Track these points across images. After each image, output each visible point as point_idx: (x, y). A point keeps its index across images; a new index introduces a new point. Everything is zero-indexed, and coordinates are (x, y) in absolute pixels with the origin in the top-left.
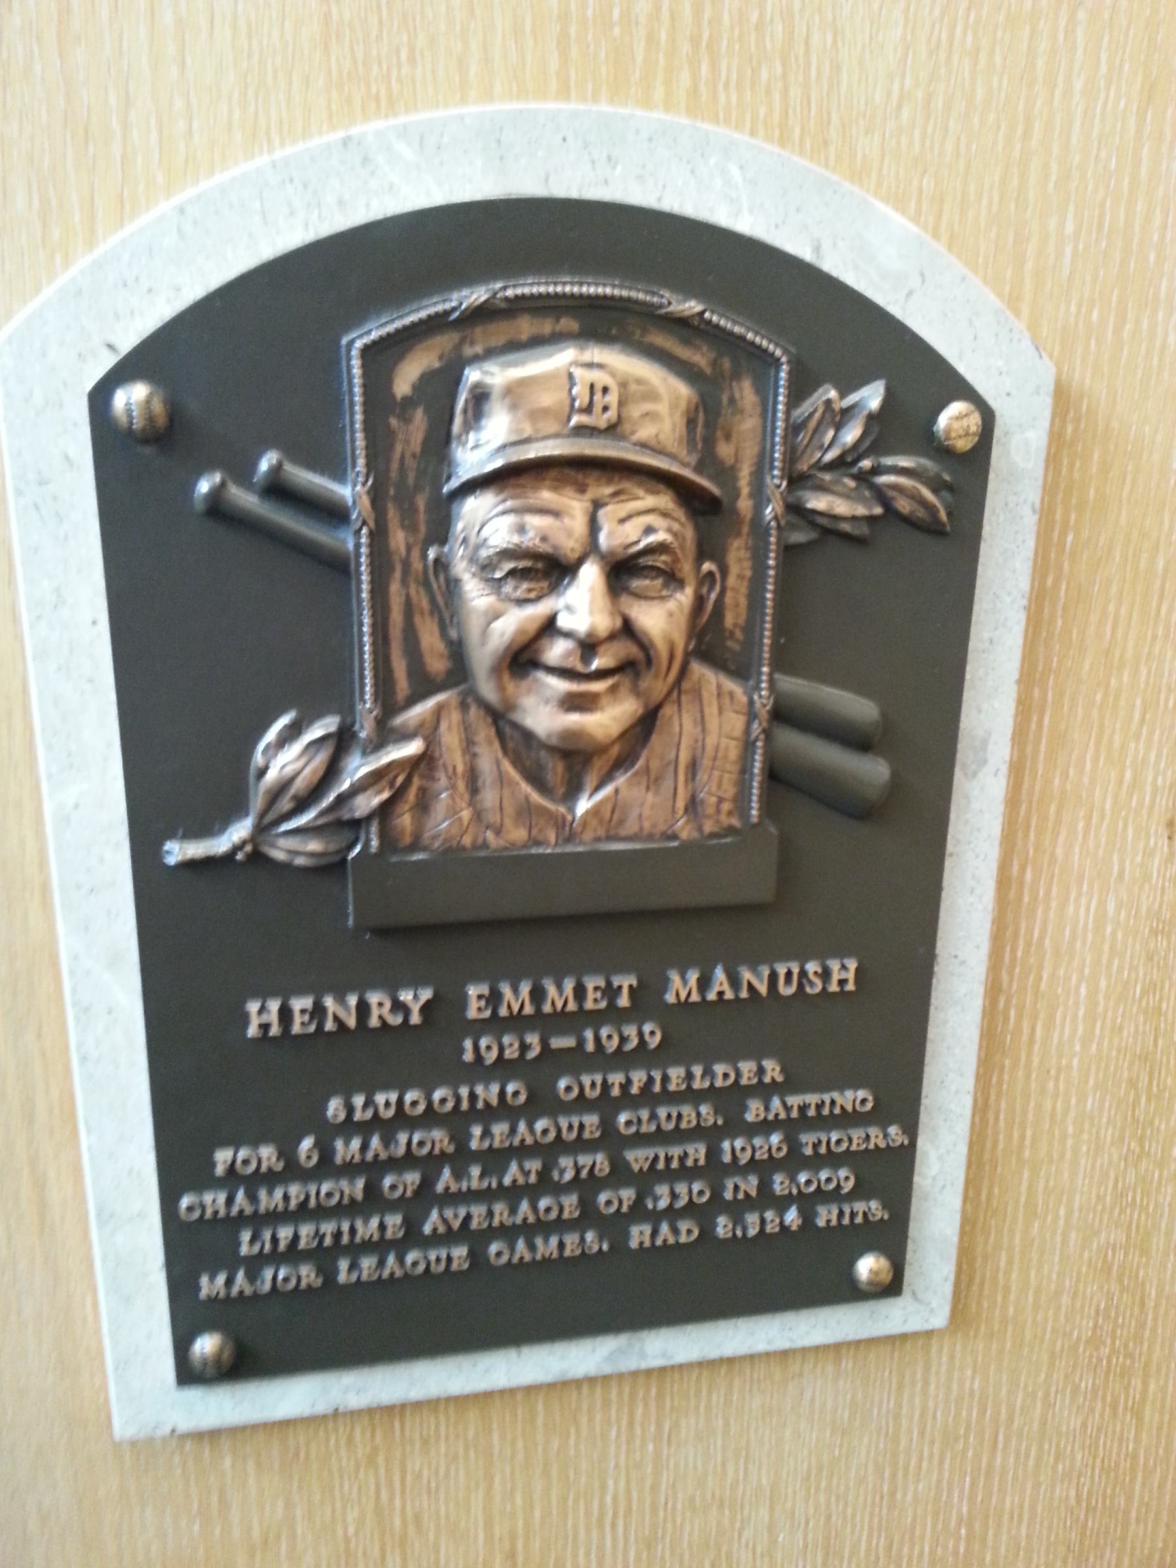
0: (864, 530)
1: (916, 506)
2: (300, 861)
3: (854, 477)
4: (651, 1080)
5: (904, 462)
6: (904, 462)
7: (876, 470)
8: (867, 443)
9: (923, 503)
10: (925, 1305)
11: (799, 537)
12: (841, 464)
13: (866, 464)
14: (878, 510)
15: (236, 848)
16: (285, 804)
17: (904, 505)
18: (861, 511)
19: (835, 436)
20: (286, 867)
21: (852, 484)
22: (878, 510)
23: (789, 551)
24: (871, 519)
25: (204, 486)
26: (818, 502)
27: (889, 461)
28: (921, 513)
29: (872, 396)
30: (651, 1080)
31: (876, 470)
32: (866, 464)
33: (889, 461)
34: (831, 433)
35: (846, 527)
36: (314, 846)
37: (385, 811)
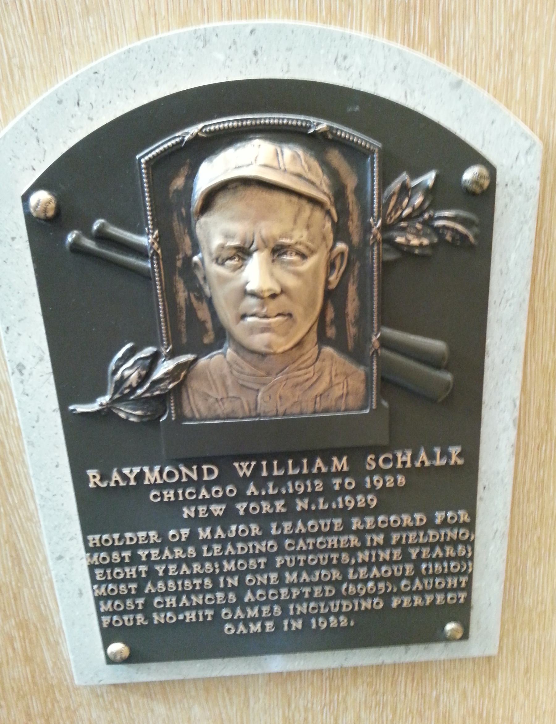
0: (428, 252)
2: (132, 419)
3: (419, 223)
4: (401, 538)
5: (447, 213)
6: (447, 213)
7: (432, 218)
10: (475, 647)
11: (390, 256)
13: (426, 216)
20: (126, 421)
21: (419, 226)
22: (436, 240)
25: (71, 238)
27: (437, 214)
30: (401, 538)
32: (426, 216)
33: (437, 214)
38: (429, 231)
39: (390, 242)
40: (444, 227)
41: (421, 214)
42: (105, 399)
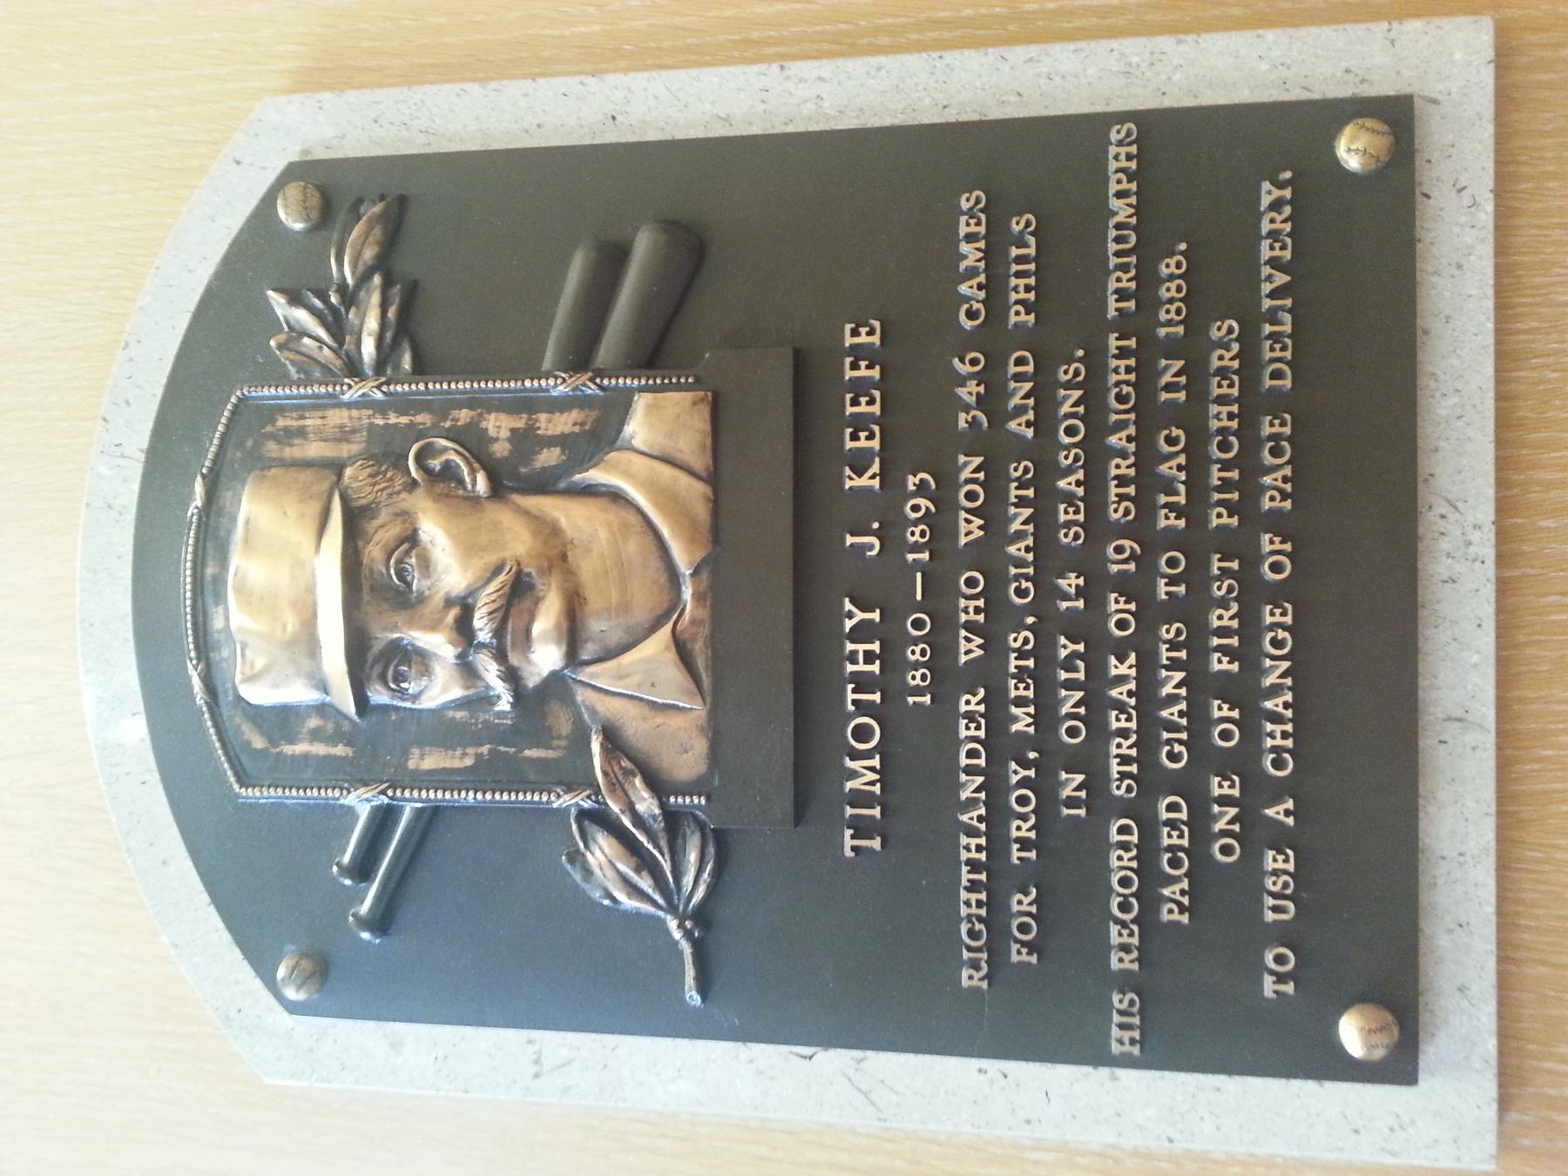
0: (396, 290)
1: (371, 239)
3: (347, 312)
8: (317, 303)
9: (367, 234)
11: (407, 362)
12: (336, 324)
13: (334, 299)
15: (688, 934)
16: (645, 883)
17: (369, 254)
18: (376, 298)
19: (310, 336)
22: (377, 279)
23: (421, 369)
24: (387, 286)
26: (368, 349)
28: (377, 232)
29: (277, 301)
31: (342, 289)
34: (306, 340)
35: (391, 314)
36: (693, 857)
37: (657, 785)
38: (362, 294)
39: (380, 366)
40: (354, 266)
42: (672, 924)
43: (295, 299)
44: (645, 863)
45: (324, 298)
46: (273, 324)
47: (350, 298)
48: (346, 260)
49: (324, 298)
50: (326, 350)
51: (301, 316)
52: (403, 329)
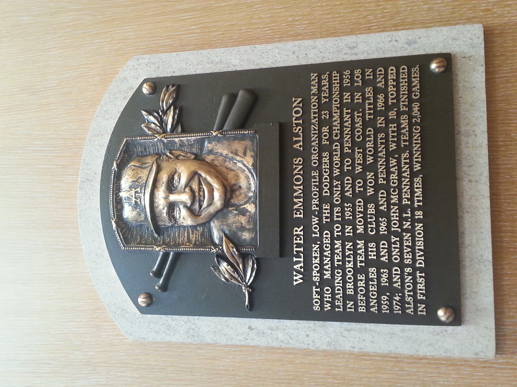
8: (156, 114)
13: (161, 114)
14: (172, 107)
16: (236, 276)
22: (172, 107)
26: (169, 126)
35: (176, 117)
40: (167, 104)
41: (160, 116)
43: (150, 114)
44: (235, 270)
45: (158, 113)
46: (143, 120)
47: (165, 113)
48: (164, 103)
49: (158, 113)
50: (158, 127)
51: (151, 118)
52: (179, 121)
